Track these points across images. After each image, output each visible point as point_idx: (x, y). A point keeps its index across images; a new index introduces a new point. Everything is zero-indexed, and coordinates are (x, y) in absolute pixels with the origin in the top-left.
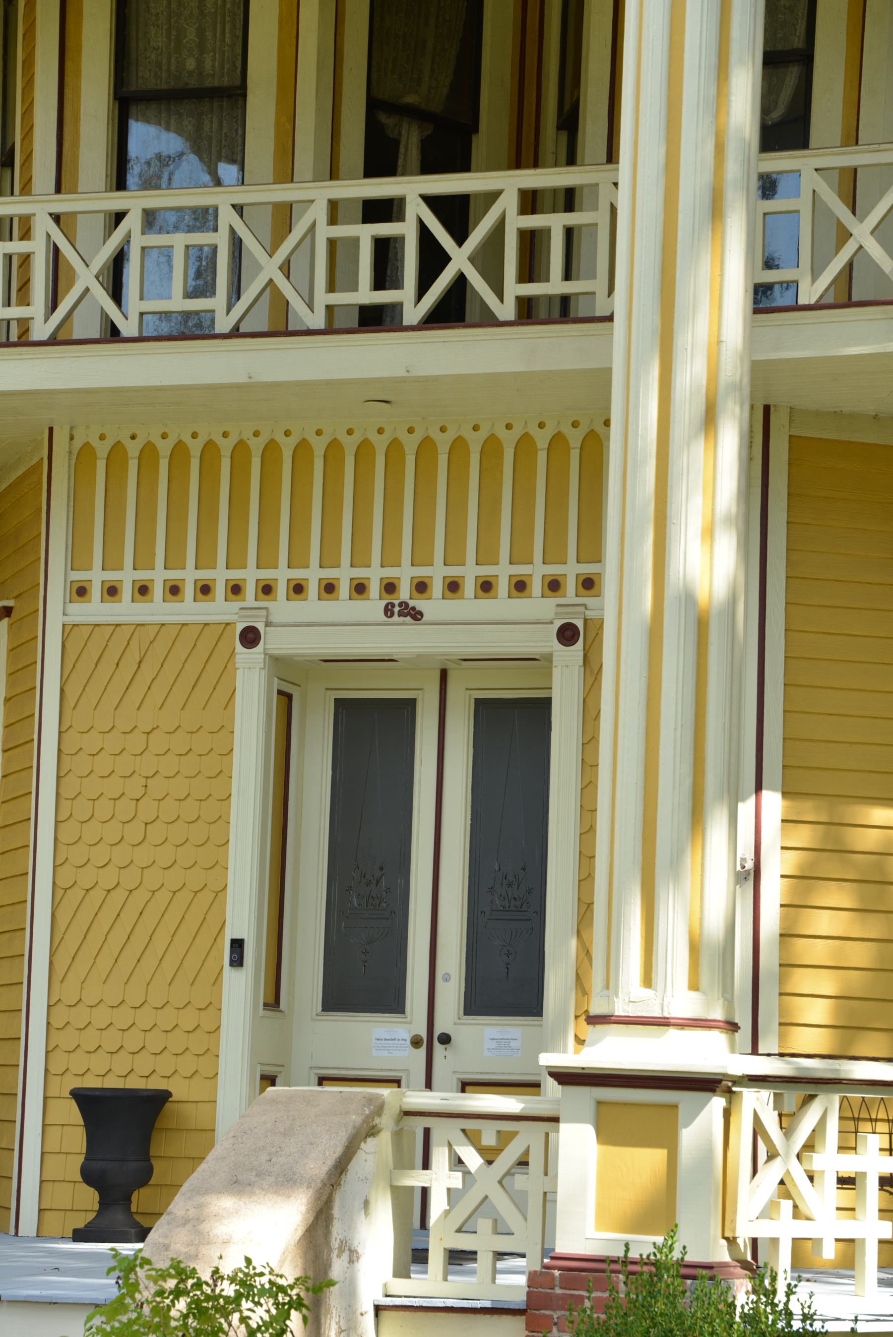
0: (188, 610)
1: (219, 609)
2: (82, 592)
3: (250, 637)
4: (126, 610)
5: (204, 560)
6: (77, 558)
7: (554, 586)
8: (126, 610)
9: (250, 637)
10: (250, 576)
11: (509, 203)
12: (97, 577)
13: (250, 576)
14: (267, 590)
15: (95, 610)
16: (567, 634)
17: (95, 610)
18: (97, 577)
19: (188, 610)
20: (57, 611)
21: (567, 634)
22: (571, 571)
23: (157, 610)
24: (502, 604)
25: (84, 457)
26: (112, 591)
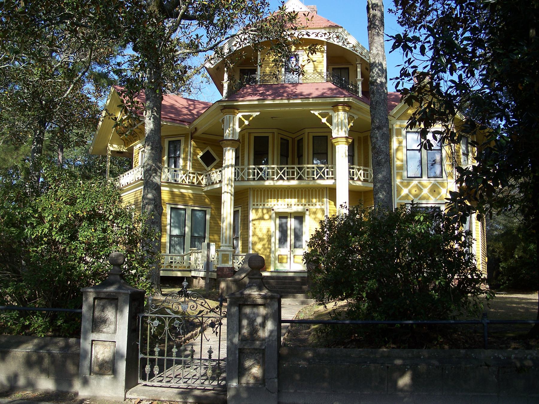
2: (254, 205)
6: (254, 201)
12: (256, 203)
18: (256, 203)
26: (257, 205)
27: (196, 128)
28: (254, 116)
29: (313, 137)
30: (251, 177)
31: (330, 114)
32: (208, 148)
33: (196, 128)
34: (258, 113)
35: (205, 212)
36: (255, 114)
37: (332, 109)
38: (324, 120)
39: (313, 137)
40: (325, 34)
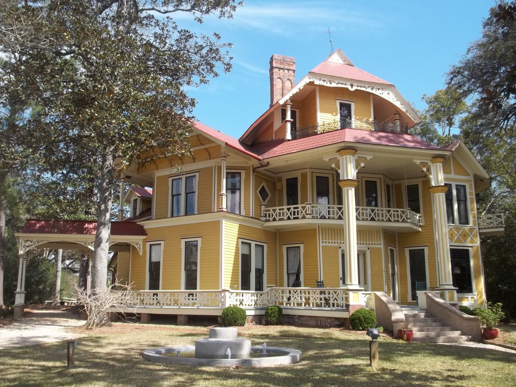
0: (333, 245)
1: (336, 245)
2: (323, 242)
3: (340, 248)
4: (327, 244)
5: (332, 240)
6: (323, 239)
7: (366, 244)
8: (327, 244)
9: (340, 248)
10: (339, 242)
11: (376, 210)
12: (324, 241)
13: (339, 242)
14: (341, 243)
15: (324, 244)
16: (368, 249)
17: (324, 244)
19: (333, 245)
20: (321, 244)
21: (368, 249)
22: (342, 242)
23: (330, 244)
24: (362, 246)
25: (322, 229)
27: (268, 163)
28: (368, 159)
29: (366, 181)
30: (331, 216)
31: (429, 164)
32: (264, 184)
33: (268, 163)
34: (371, 157)
35: (263, 246)
36: (369, 158)
37: (431, 160)
38: (425, 169)
39: (366, 181)
40: (379, 89)
